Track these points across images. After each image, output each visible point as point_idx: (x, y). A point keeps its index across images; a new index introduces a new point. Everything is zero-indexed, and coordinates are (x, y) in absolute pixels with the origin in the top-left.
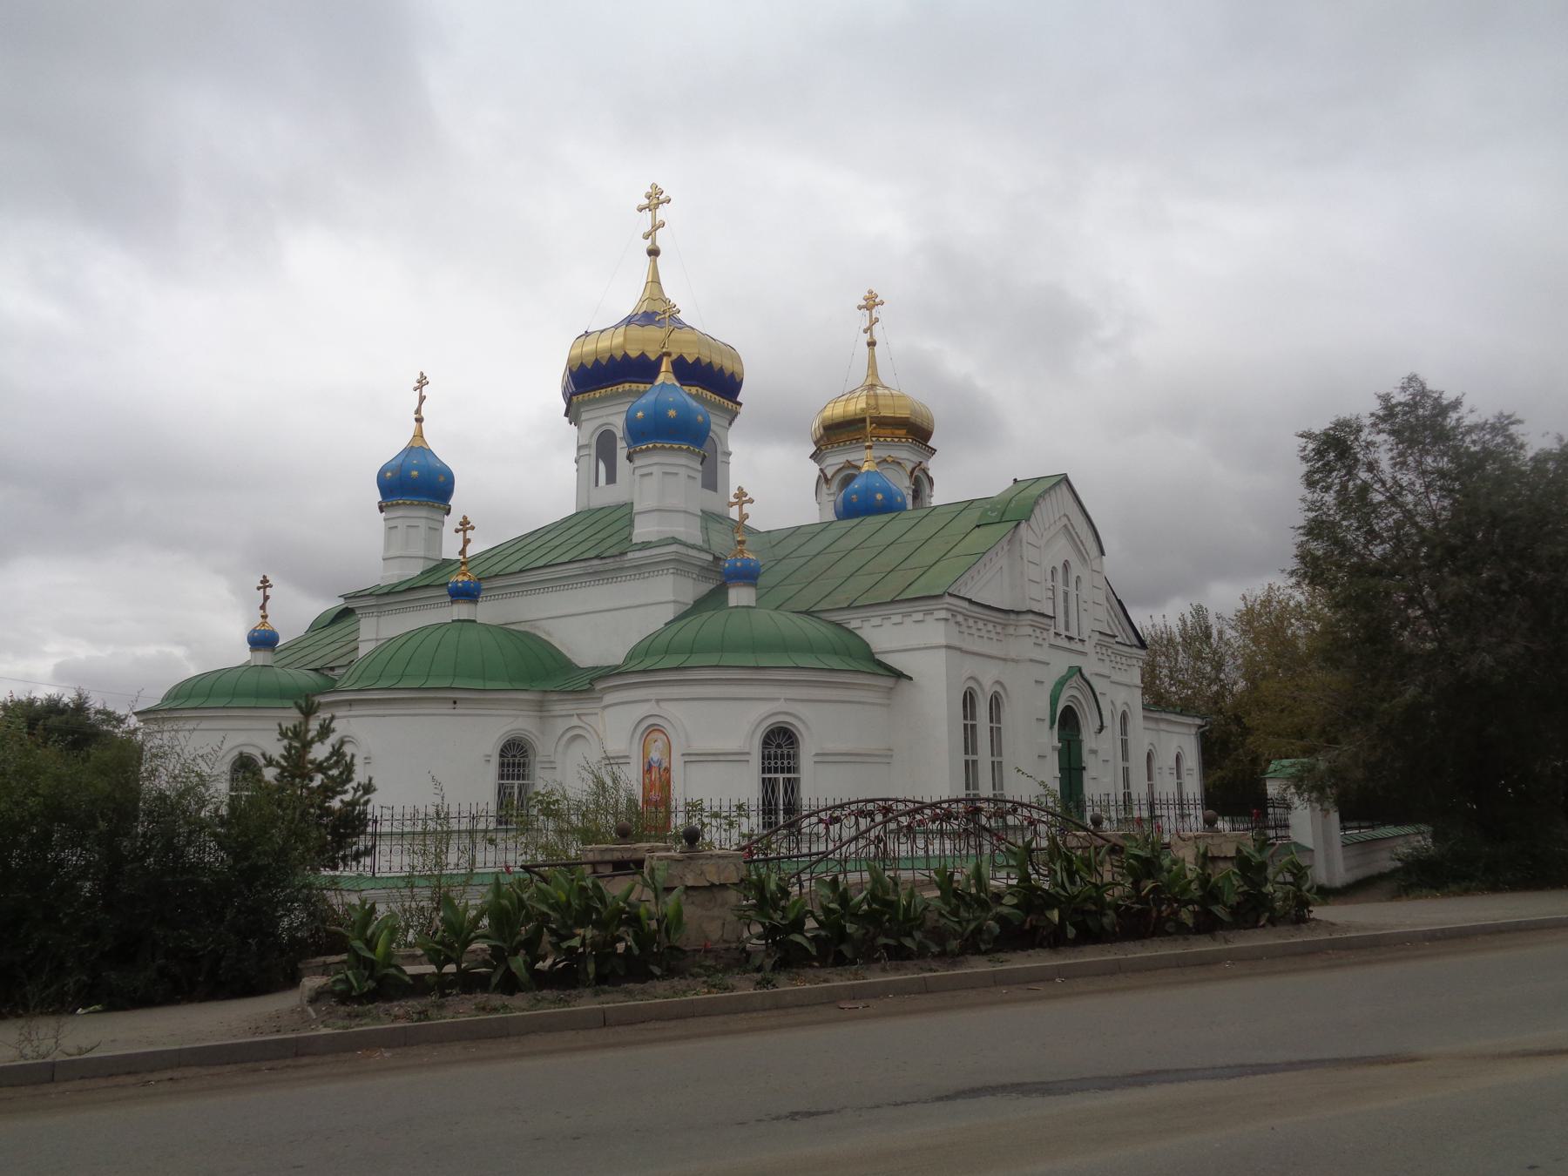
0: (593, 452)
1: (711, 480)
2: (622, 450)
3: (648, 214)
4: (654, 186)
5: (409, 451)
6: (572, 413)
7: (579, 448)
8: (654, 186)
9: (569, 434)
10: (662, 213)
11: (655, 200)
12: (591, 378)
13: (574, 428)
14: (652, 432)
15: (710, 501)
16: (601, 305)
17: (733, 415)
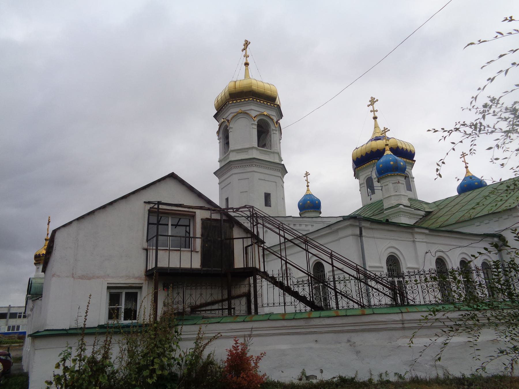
0: (365, 185)
1: (410, 187)
2: (376, 184)
3: (371, 107)
4: (372, 98)
5: (306, 195)
6: (356, 176)
7: (360, 185)
8: (372, 98)
9: (356, 182)
10: (376, 106)
11: (373, 101)
12: (361, 161)
13: (357, 181)
14: (384, 172)
15: (410, 194)
16: (362, 138)
17: (412, 165)
